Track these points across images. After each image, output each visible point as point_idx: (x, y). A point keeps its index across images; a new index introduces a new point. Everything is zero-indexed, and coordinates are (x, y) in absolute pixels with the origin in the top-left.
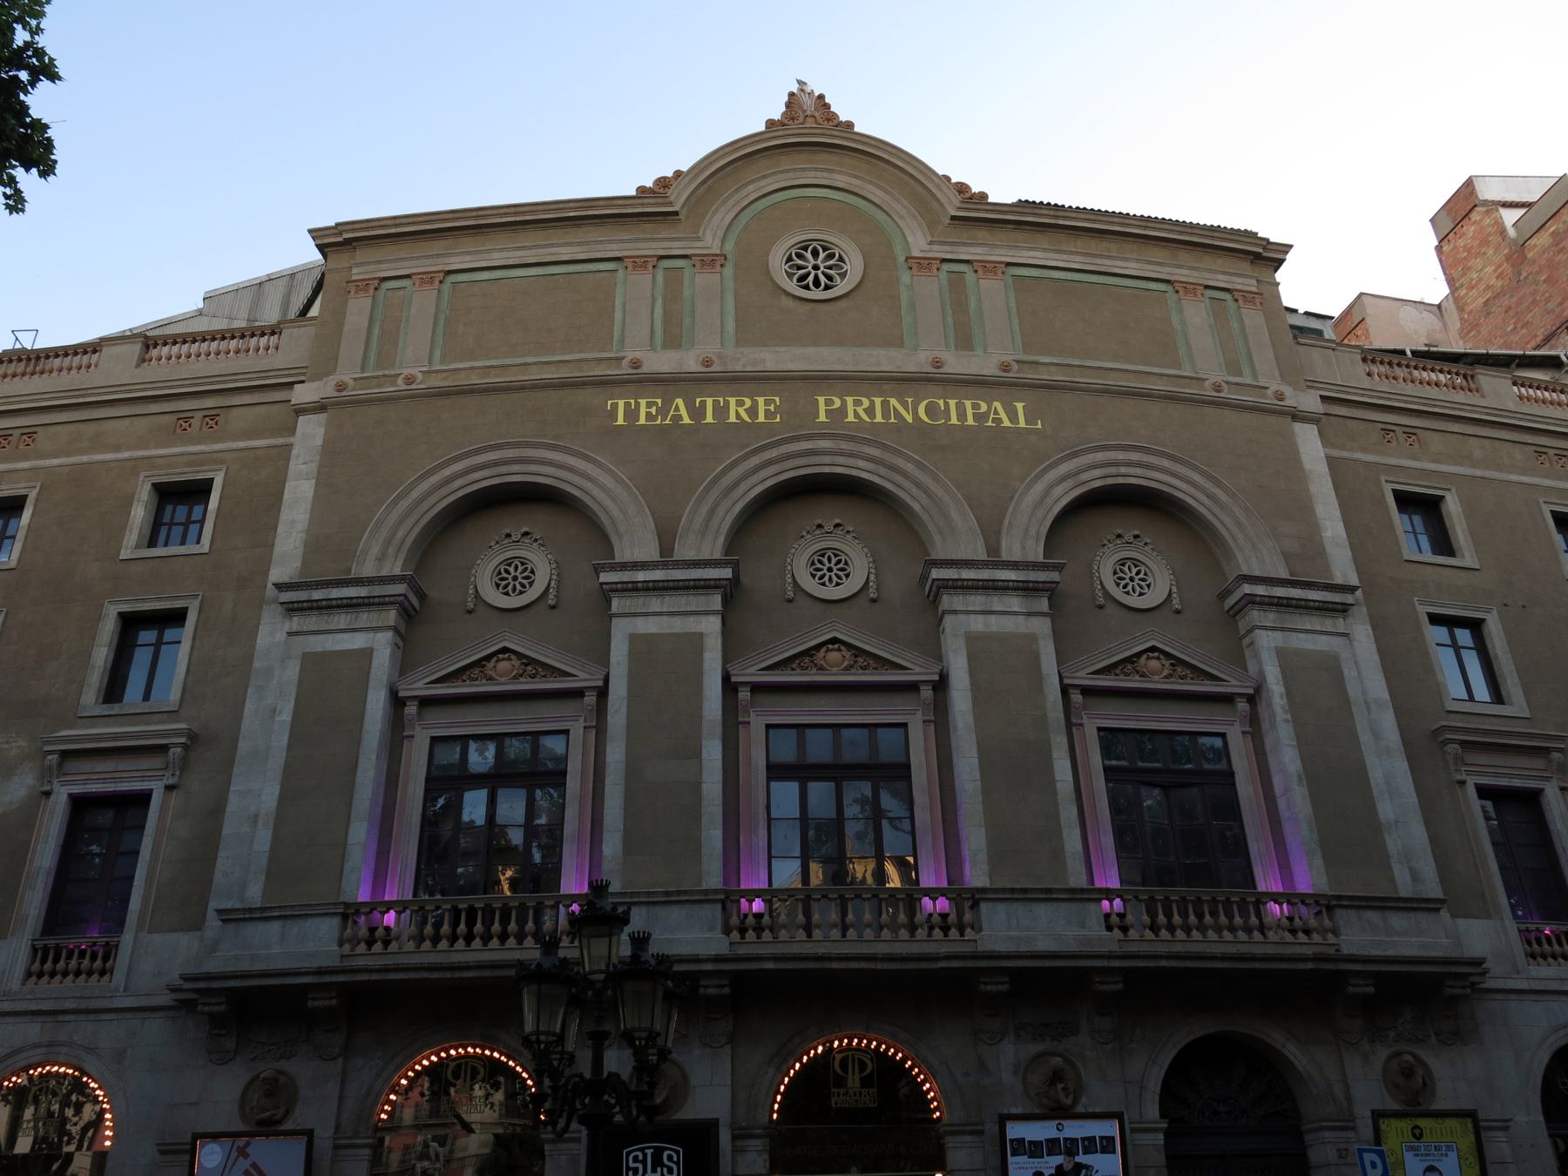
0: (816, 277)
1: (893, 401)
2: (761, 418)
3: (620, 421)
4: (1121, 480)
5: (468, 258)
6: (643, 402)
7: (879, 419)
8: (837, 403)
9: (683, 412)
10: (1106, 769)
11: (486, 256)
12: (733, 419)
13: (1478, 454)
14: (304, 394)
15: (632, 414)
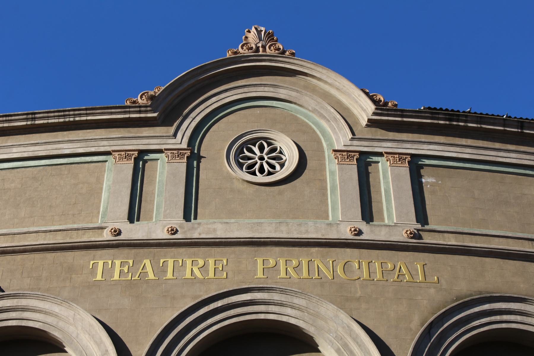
0: (262, 167)
1: (317, 262)
2: (211, 275)
3: (99, 277)
4: (504, 326)
6: (118, 263)
7: (305, 274)
8: (272, 262)
9: (149, 269)
11: (8, 150)
15: (108, 271)
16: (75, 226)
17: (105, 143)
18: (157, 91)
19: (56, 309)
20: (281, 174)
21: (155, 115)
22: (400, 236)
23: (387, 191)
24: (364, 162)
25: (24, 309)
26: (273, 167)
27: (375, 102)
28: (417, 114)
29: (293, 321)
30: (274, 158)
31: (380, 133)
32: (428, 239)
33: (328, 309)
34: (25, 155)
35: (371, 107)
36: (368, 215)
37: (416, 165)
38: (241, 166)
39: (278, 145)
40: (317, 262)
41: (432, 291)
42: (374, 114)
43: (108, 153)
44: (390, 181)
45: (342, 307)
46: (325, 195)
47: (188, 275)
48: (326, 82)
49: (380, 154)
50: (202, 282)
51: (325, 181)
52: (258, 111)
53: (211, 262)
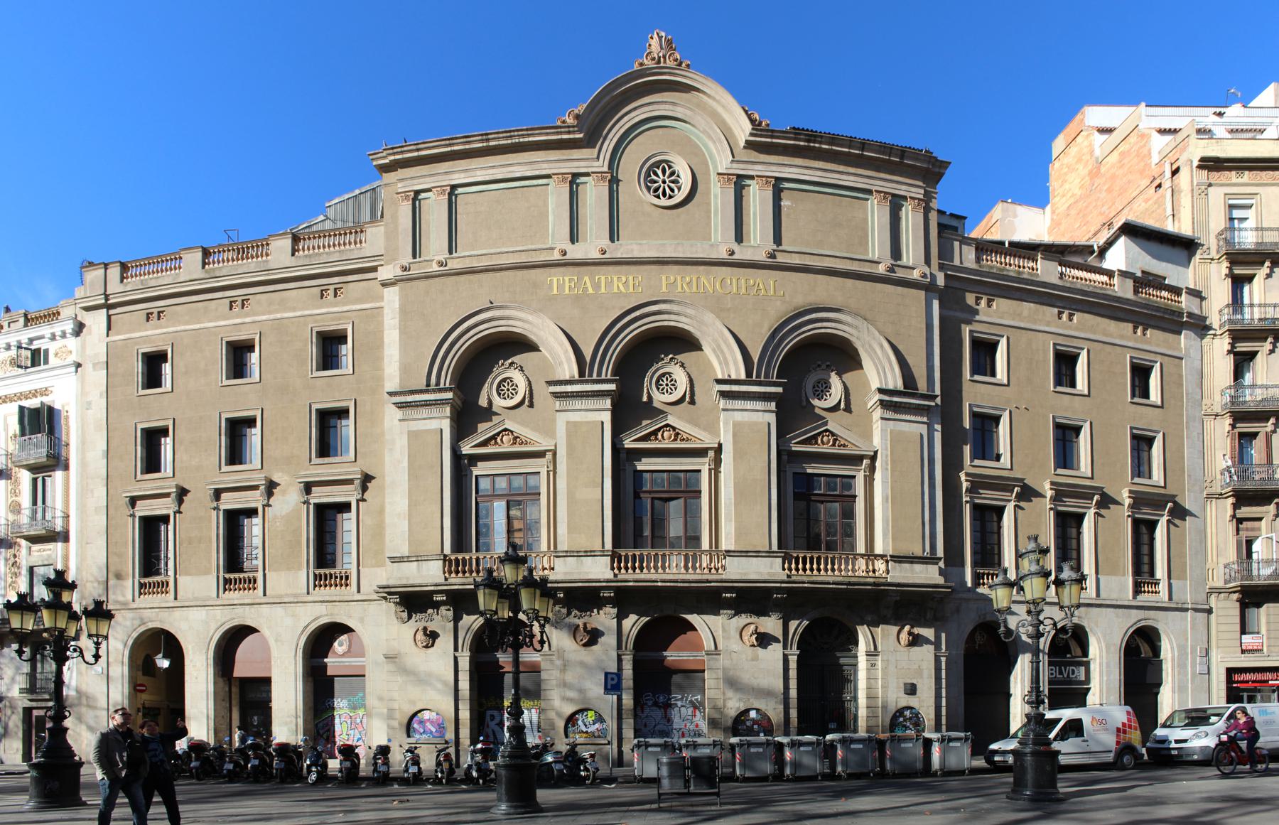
5: (462, 175)
6: (567, 279)
7: (694, 289)
9: (589, 284)
10: (795, 494)
12: (616, 290)
13: (1026, 313)
14: (385, 273)
16: (533, 247)
17: (545, 166)
18: (580, 109)
19: (530, 318)
20: (680, 197)
21: (581, 136)
22: (761, 256)
23: (755, 214)
24: (740, 183)
25: (509, 318)
26: (672, 190)
27: (752, 121)
28: (784, 134)
29: (686, 327)
30: (673, 182)
31: (754, 156)
32: (781, 258)
33: (709, 317)
34: (487, 178)
35: (748, 127)
36: (739, 238)
37: (778, 187)
38: (648, 188)
39: (676, 168)
40: (703, 279)
41: (779, 303)
42: (751, 135)
43: (548, 176)
44: (758, 199)
45: (718, 317)
46: (709, 217)
47: (616, 290)
48: (714, 99)
49: (752, 177)
50: (626, 295)
51: (709, 204)
52: (660, 131)
53: (631, 278)
